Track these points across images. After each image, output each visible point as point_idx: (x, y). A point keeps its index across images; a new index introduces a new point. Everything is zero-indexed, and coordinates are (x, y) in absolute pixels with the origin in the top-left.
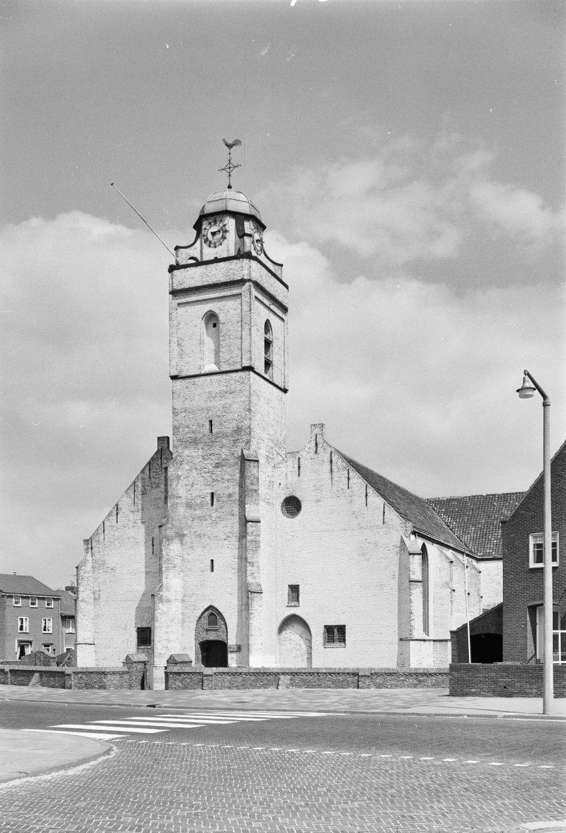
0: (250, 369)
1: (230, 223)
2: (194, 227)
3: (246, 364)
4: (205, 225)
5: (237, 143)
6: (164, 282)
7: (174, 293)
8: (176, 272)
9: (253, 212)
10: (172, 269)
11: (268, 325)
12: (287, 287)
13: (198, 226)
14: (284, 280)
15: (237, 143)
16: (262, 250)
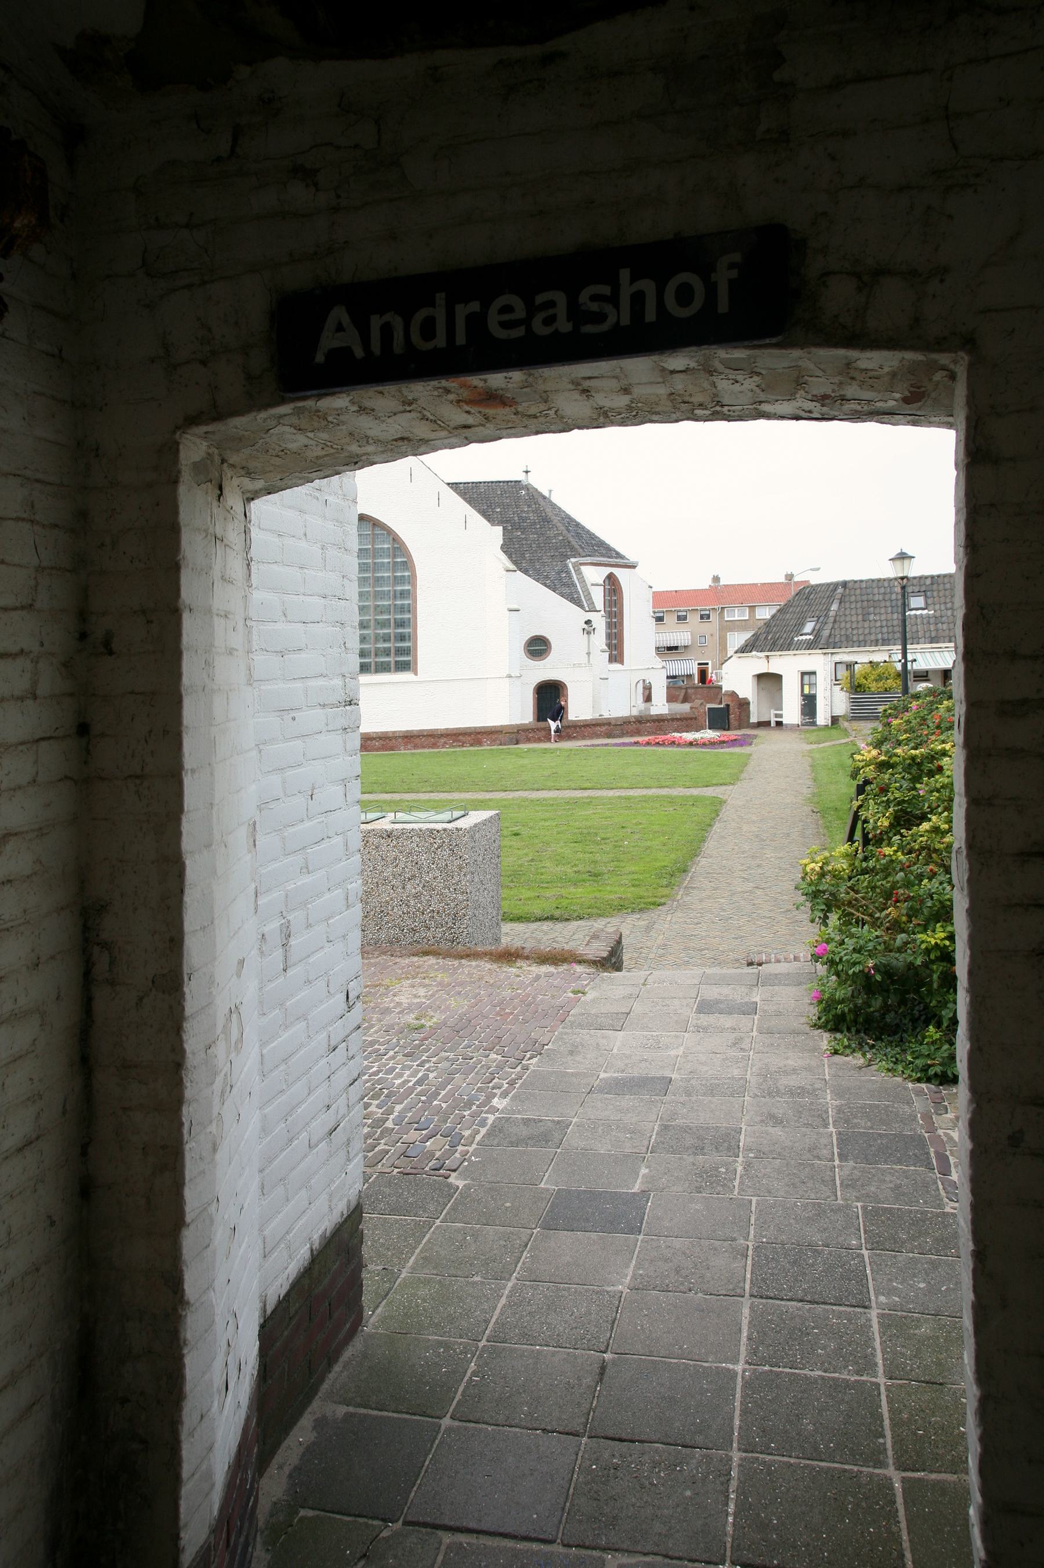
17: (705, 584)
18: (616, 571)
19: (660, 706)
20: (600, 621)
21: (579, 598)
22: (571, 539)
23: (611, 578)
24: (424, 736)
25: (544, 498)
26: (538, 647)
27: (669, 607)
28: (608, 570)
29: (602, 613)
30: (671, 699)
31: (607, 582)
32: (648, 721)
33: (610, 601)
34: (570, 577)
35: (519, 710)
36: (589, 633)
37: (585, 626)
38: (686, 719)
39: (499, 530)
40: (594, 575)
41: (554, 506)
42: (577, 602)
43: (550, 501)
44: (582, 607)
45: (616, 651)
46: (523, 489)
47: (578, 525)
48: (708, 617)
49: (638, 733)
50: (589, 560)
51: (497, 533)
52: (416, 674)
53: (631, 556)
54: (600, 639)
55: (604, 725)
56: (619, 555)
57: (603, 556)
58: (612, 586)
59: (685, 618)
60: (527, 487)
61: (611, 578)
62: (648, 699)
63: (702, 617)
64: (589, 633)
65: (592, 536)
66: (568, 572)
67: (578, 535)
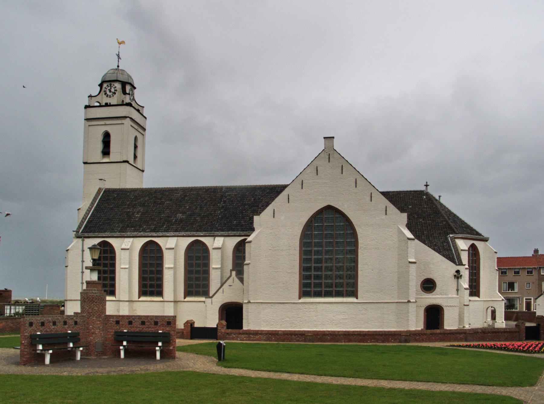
0: (127, 162)
1: (118, 86)
2: (99, 85)
3: (125, 159)
4: (105, 85)
5: (123, 42)
6: (82, 114)
7: (87, 120)
8: (88, 109)
9: (130, 82)
10: (86, 107)
11: (136, 138)
12: (146, 118)
13: (101, 85)
14: (144, 115)
15: (123, 42)
16: (134, 99)
17: (530, 253)
18: (476, 243)
19: (501, 323)
20: (465, 274)
21: (453, 257)
22: (451, 223)
23: (473, 247)
24: (355, 335)
25: (436, 200)
26: (429, 285)
27: (505, 266)
28: (472, 242)
29: (467, 266)
30: (508, 317)
31: (471, 249)
32: (489, 332)
33: (472, 260)
34: (449, 246)
35: (416, 323)
36: (458, 278)
37: (456, 274)
38: (512, 332)
39: (405, 215)
40: (463, 245)
41: (441, 205)
42: (452, 260)
43: (440, 202)
44: (454, 262)
45: (474, 290)
46: (424, 195)
47: (455, 216)
48: (531, 272)
49: (483, 339)
50: (460, 236)
51: (404, 217)
52: (357, 298)
53: (485, 235)
54: (465, 283)
55: (462, 333)
56: (480, 235)
57: (469, 234)
58: (474, 251)
59: (518, 273)
60: (427, 194)
61: (473, 247)
62: (494, 317)
63: (528, 272)
64: (458, 278)
65: (463, 222)
66: (448, 242)
67: (454, 222)
